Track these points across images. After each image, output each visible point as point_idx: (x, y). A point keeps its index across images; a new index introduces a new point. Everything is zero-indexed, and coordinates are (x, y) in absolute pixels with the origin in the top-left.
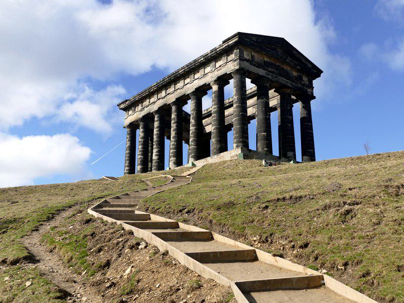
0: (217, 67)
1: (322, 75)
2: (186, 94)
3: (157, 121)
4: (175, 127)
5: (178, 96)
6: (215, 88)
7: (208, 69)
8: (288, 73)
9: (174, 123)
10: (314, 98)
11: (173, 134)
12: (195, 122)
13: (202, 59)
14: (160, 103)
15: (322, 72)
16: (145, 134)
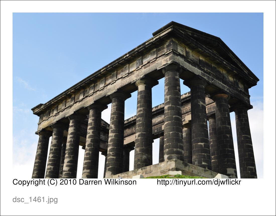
0: (144, 64)
1: (258, 83)
2: (107, 95)
3: (72, 126)
4: (91, 134)
5: (97, 98)
6: (141, 87)
8: (224, 77)
9: (90, 129)
10: (251, 107)
11: (88, 141)
12: (115, 127)
13: (128, 55)
14: (77, 106)
16: (57, 142)
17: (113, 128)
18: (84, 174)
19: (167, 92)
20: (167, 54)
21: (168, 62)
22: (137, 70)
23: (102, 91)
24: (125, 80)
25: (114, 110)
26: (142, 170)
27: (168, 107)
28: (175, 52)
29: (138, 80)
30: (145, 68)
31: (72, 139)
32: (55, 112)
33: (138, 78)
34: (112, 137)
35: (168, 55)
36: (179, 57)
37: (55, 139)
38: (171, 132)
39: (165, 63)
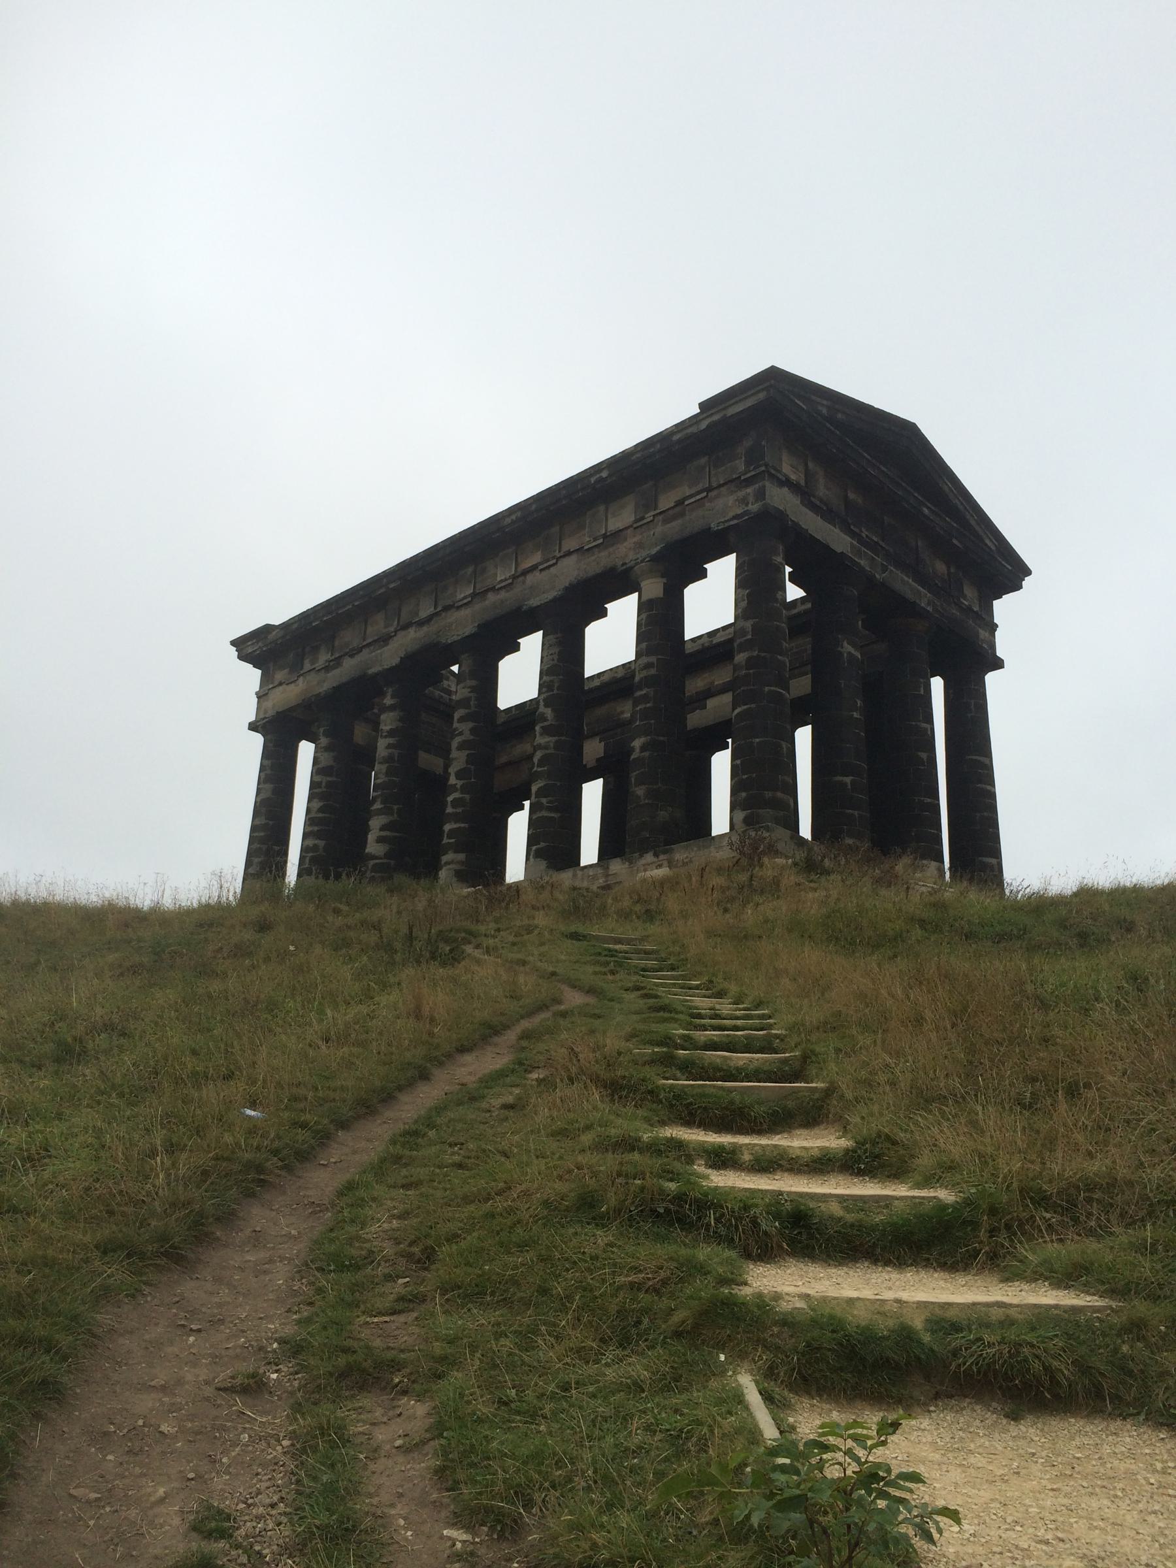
1: (1027, 582)
4: (467, 736)
7: (622, 517)
10: (998, 664)
14: (408, 640)
15: (1028, 572)
17: (549, 718)
18: (448, 867)
19: (745, 611)
20: (745, 480)
21: (750, 505)
22: (635, 526)
23: (508, 591)
24: (593, 558)
25: (553, 660)
26: (656, 855)
27: (749, 659)
28: (773, 472)
29: (642, 562)
30: (665, 522)
31: (396, 752)
32: (323, 658)
33: (644, 554)
34: (546, 748)
35: (748, 482)
36: (786, 489)
37: (327, 749)
38: (757, 740)
39: (739, 511)
